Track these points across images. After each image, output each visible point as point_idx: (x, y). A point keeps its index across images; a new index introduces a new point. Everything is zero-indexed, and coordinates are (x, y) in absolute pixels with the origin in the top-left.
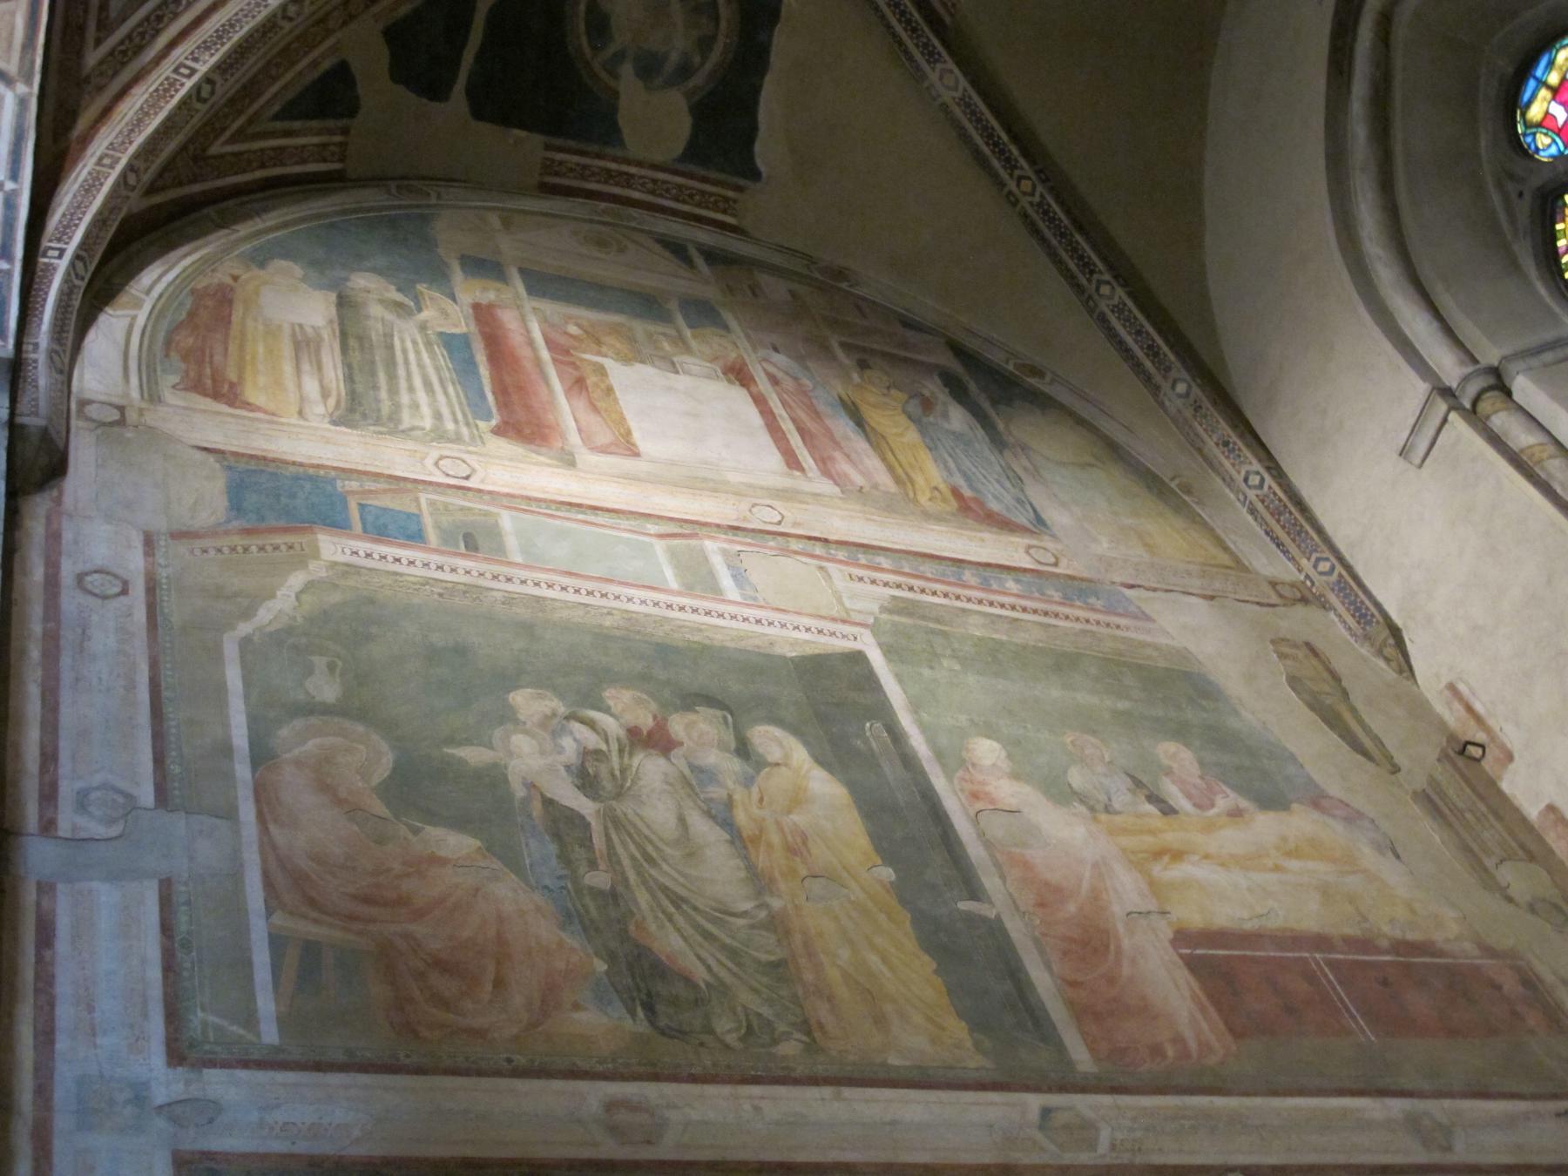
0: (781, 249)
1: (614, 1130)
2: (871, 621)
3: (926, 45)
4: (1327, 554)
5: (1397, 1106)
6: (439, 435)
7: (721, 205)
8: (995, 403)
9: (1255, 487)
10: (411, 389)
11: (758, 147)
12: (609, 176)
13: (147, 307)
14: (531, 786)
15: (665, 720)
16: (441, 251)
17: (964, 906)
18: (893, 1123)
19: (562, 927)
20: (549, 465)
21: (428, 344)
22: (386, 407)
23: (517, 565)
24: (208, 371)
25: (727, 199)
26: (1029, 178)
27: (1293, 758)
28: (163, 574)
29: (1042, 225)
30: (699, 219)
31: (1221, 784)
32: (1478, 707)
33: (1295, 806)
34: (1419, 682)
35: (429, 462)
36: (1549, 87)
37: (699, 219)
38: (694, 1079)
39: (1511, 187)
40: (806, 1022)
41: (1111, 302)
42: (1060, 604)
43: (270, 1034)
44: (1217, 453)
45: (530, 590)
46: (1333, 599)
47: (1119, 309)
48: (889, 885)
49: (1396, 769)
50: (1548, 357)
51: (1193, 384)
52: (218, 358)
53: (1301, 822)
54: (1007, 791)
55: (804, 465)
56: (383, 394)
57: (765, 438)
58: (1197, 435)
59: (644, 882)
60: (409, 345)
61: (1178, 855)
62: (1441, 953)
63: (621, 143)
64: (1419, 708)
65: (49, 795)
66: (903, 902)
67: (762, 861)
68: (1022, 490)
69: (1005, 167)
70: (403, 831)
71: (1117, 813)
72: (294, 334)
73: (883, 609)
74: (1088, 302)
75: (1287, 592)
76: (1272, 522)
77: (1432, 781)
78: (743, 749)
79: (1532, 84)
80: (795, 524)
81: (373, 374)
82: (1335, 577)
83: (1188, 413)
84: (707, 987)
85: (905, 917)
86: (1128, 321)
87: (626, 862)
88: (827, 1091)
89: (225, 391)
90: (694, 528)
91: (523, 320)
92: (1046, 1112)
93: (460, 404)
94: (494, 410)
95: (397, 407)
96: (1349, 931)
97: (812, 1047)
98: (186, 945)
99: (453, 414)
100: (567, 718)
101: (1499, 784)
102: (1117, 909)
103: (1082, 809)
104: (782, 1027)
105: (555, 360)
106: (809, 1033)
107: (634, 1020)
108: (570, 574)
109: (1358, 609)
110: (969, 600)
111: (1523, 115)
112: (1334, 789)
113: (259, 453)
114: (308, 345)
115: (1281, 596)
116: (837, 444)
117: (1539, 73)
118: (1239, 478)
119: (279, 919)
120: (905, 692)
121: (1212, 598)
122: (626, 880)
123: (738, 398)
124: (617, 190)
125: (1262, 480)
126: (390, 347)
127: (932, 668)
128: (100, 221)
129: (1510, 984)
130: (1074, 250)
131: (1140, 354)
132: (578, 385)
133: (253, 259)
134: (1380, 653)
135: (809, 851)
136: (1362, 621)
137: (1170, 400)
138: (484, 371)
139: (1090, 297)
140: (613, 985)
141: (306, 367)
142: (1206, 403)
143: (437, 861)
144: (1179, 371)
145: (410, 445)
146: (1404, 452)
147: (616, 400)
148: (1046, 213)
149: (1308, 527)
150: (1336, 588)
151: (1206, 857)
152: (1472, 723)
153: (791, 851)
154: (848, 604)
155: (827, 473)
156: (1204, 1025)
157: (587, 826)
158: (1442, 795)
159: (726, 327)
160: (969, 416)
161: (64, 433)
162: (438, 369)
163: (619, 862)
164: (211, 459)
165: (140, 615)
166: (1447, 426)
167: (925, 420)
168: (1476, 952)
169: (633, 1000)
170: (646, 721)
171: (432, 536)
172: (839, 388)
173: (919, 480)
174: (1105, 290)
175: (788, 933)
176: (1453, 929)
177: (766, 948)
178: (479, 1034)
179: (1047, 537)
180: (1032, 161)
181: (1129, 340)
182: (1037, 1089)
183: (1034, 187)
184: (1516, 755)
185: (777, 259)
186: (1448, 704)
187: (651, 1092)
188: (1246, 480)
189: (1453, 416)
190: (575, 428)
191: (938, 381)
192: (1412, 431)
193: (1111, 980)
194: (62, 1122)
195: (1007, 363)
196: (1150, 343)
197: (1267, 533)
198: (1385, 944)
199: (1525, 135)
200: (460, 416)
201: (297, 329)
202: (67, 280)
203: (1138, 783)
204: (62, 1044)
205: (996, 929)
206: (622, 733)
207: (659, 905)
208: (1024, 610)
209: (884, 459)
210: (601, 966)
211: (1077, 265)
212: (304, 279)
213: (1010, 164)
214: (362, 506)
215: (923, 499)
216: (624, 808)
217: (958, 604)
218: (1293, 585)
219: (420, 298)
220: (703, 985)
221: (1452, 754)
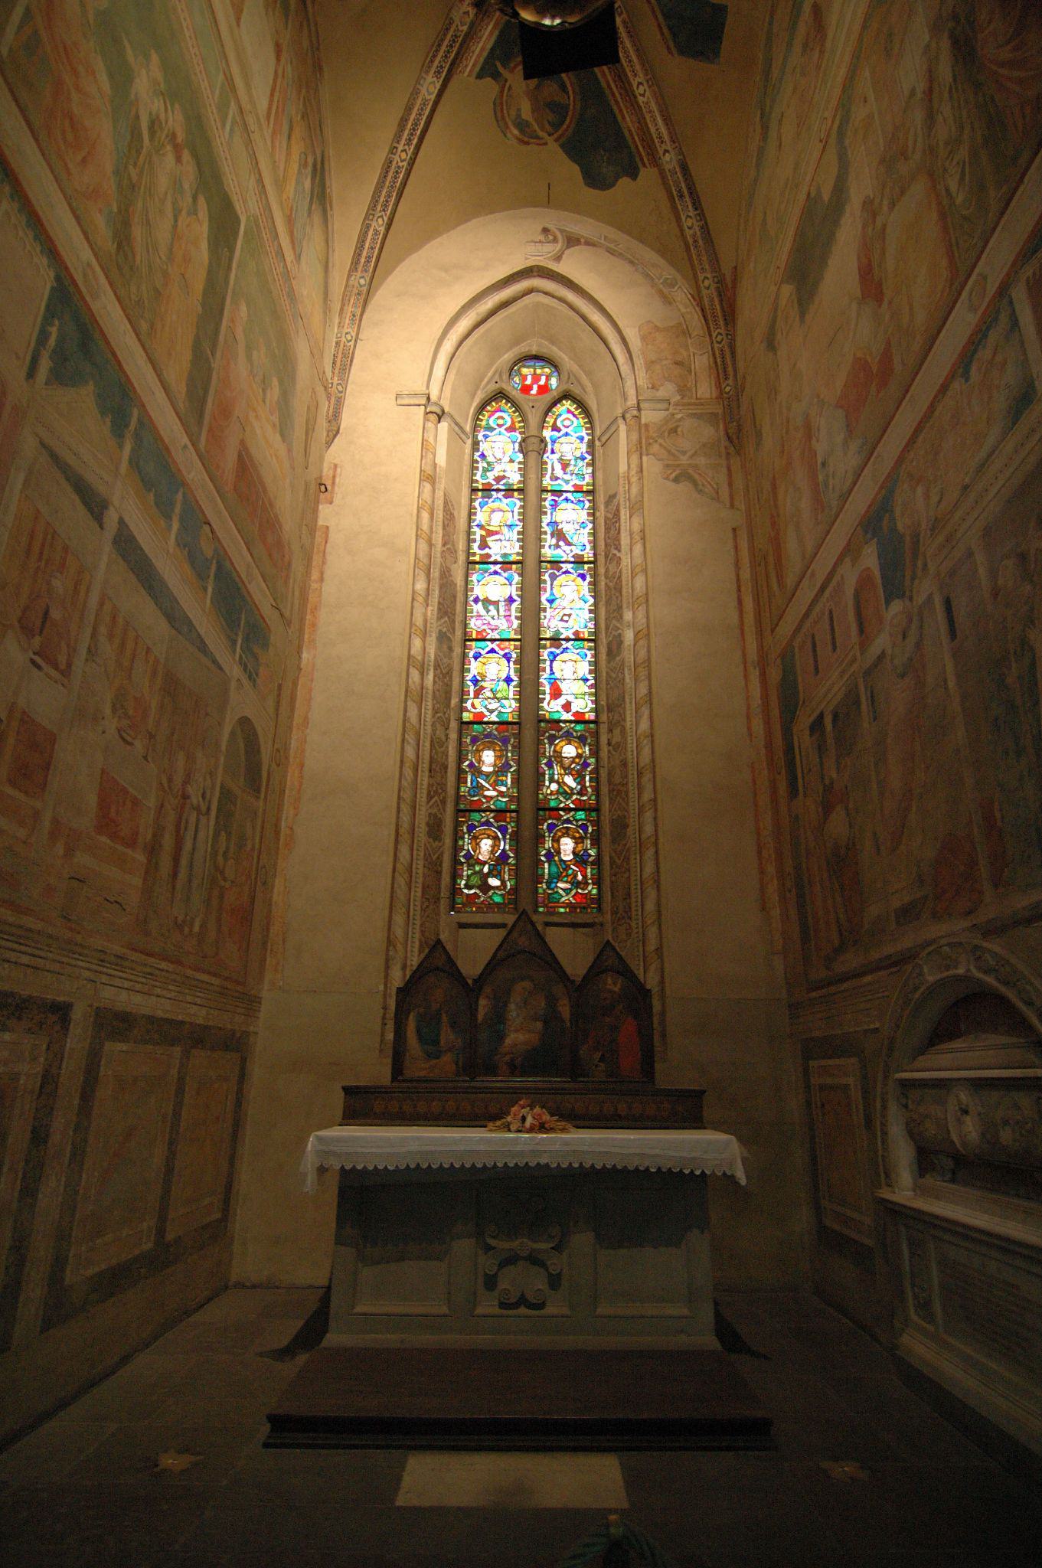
3: (441, 67)
29: (391, 174)
32: (337, 480)
36: (535, 371)
39: (497, 378)
46: (333, 399)
47: (376, 232)
50: (456, 428)
76: (340, 355)
79: (532, 364)
111: (521, 367)
134: (328, 432)
146: (398, 396)
186: (330, 468)
188: (347, 334)
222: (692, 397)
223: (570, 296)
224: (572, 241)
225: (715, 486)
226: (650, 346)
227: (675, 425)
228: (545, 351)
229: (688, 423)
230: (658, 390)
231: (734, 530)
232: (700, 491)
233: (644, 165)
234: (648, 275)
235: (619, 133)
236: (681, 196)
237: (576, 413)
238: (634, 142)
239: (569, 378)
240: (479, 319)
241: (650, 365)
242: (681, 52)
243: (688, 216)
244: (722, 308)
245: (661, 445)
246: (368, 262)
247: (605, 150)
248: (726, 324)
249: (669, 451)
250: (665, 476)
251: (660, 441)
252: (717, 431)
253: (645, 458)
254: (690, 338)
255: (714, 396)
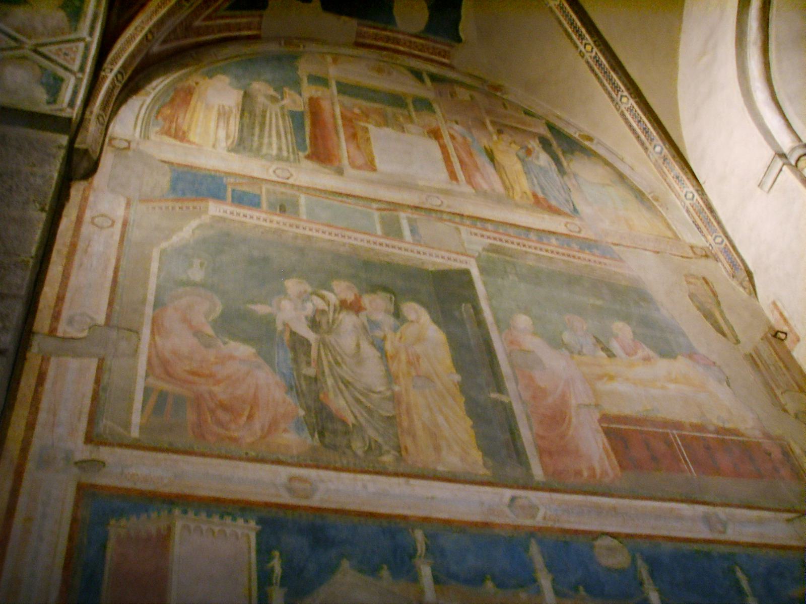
0: (471, 76)
1: (290, 490)
2: (477, 254)
4: (721, 234)
5: (701, 509)
6: (279, 158)
7: (443, 54)
8: (564, 152)
9: (690, 199)
10: (270, 136)
11: (461, 27)
12: (388, 39)
13: (152, 96)
14: (286, 325)
15: (360, 296)
16: (299, 72)
17: (494, 395)
18: (432, 498)
19: (287, 393)
20: (328, 174)
21: (283, 115)
22: (255, 145)
23: (304, 221)
24: (174, 125)
25: (445, 51)
26: (589, 44)
27: (684, 335)
28: (131, 218)
29: (596, 68)
30: (432, 61)
31: (642, 344)
32: (786, 314)
33: (679, 357)
34: (760, 300)
35: (271, 171)
37: (432, 61)
38: (336, 469)
40: (399, 447)
41: (627, 106)
42: (578, 251)
43: (135, 433)
44: (673, 182)
45: (308, 232)
46: (722, 257)
47: (630, 109)
48: (457, 384)
49: (738, 342)
51: (664, 147)
52: (180, 121)
53: (681, 365)
54: (532, 343)
55: (459, 179)
56: (256, 139)
57: (442, 165)
58: (664, 173)
59: (333, 375)
60: (274, 116)
61: (611, 378)
62: (743, 435)
63: (395, 23)
64: (757, 313)
65: (56, 317)
66: (463, 392)
67: (394, 367)
68: (570, 196)
69: (579, 39)
70: (220, 343)
71: (584, 355)
72: (219, 109)
73: (484, 249)
74: (617, 106)
75: (698, 251)
77: (757, 350)
78: (397, 314)
80: (448, 207)
81: (253, 128)
82: (723, 245)
83: (661, 161)
84: (353, 427)
85: (462, 400)
86: (635, 116)
87: (325, 363)
88: (402, 480)
89: (180, 135)
90: (395, 206)
91: (333, 104)
92: (513, 499)
93: (292, 144)
94: (308, 147)
95: (261, 145)
96: (695, 421)
97: (400, 458)
98: (105, 390)
99: (288, 148)
100: (312, 294)
101: (792, 352)
102: (573, 402)
103: (567, 353)
104: (385, 448)
105: (344, 125)
106: (400, 452)
107: (313, 439)
108: (329, 226)
109: (732, 262)
110: (530, 247)
112: (702, 350)
113: (190, 164)
114: (224, 115)
115: (694, 253)
116: (477, 167)
118: (682, 195)
119: (151, 380)
120: (487, 291)
121: (658, 252)
122: (324, 372)
123: (433, 146)
124: (392, 46)
125: (693, 196)
126: (264, 117)
127: (502, 278)
128: (133, 56)
129: (776, 454)
130: (610, 80)
131: (639, 131)
132: (353, 136)
133: (207, 75)
134: (741, 284)
135: (419, 364)
136: (734, 268)
137: (652, 155)
138: (308, 129)
139: (617, 103)
140: (305, 420)
141: (221, 124)
142: (669, 157)
143: (231, 357)
144: (657, 140)
145: (264, 162)
147: (370, 144)
148: (597, 61)
149: (713, 220)
150: (723, 251)
151: (627, 379)
152: (782, 322)
153: (409, 363)
154: (466, 245)
155: (470, 181)
156: (607, 463)
157: (310, 345)
158: (759, 356)
159: (434, 112)
160: (550, 159)
161: (98, 153)
162: (285, 128)
163: (322, 364)
164: (166, 166)
165: (117, 237)
166: (782, 173)
167: (526, 159)
168: (761, 436)
169: (314, 429)
170: (350, 297)
171: (264, 205)
172: (485, 142)
173: (517, 187)
174: (624, 100)
175: (399, 403)
176: (751, 424)
177: (387, 410)
178: (234, 440)
179: (577, 219)
180: (592, 36)
181: (634, 125)
182: (511, 487)
183: (592, 48)
184: (801, 339)
185: (468, 81)
186: (772, 311)
187: (312, 473)
188: (686, 196)
189: (785, 168)
190: (347, 156)
191: (538, 142)
192: (765, 175)
193: (562, 437)
194: (30, 466)
195: (575, 133)
196: (644, 126)
197: (693, 222)
198: (712, 428)
200: (291, 150)
201: (221, 107)
202: (113, 82)
203: (598, 341)
204: (38, 429)
205: (507, 410)
206: (337, 303)
207: (338, 386)
208: (558, 253)
209: (501, 178)
210: (302, 413)
211: (612, 88)
212: (230, 84)
213: (581, 37)
214: (233, 191)
215: (517, 198)
216: (330, 338)
217: (524, 249)
218: (702, 248)
219: (284, 94)
220: (351, 425)
221: (769, 336)
240: (759, 44)
246: (647, 132)
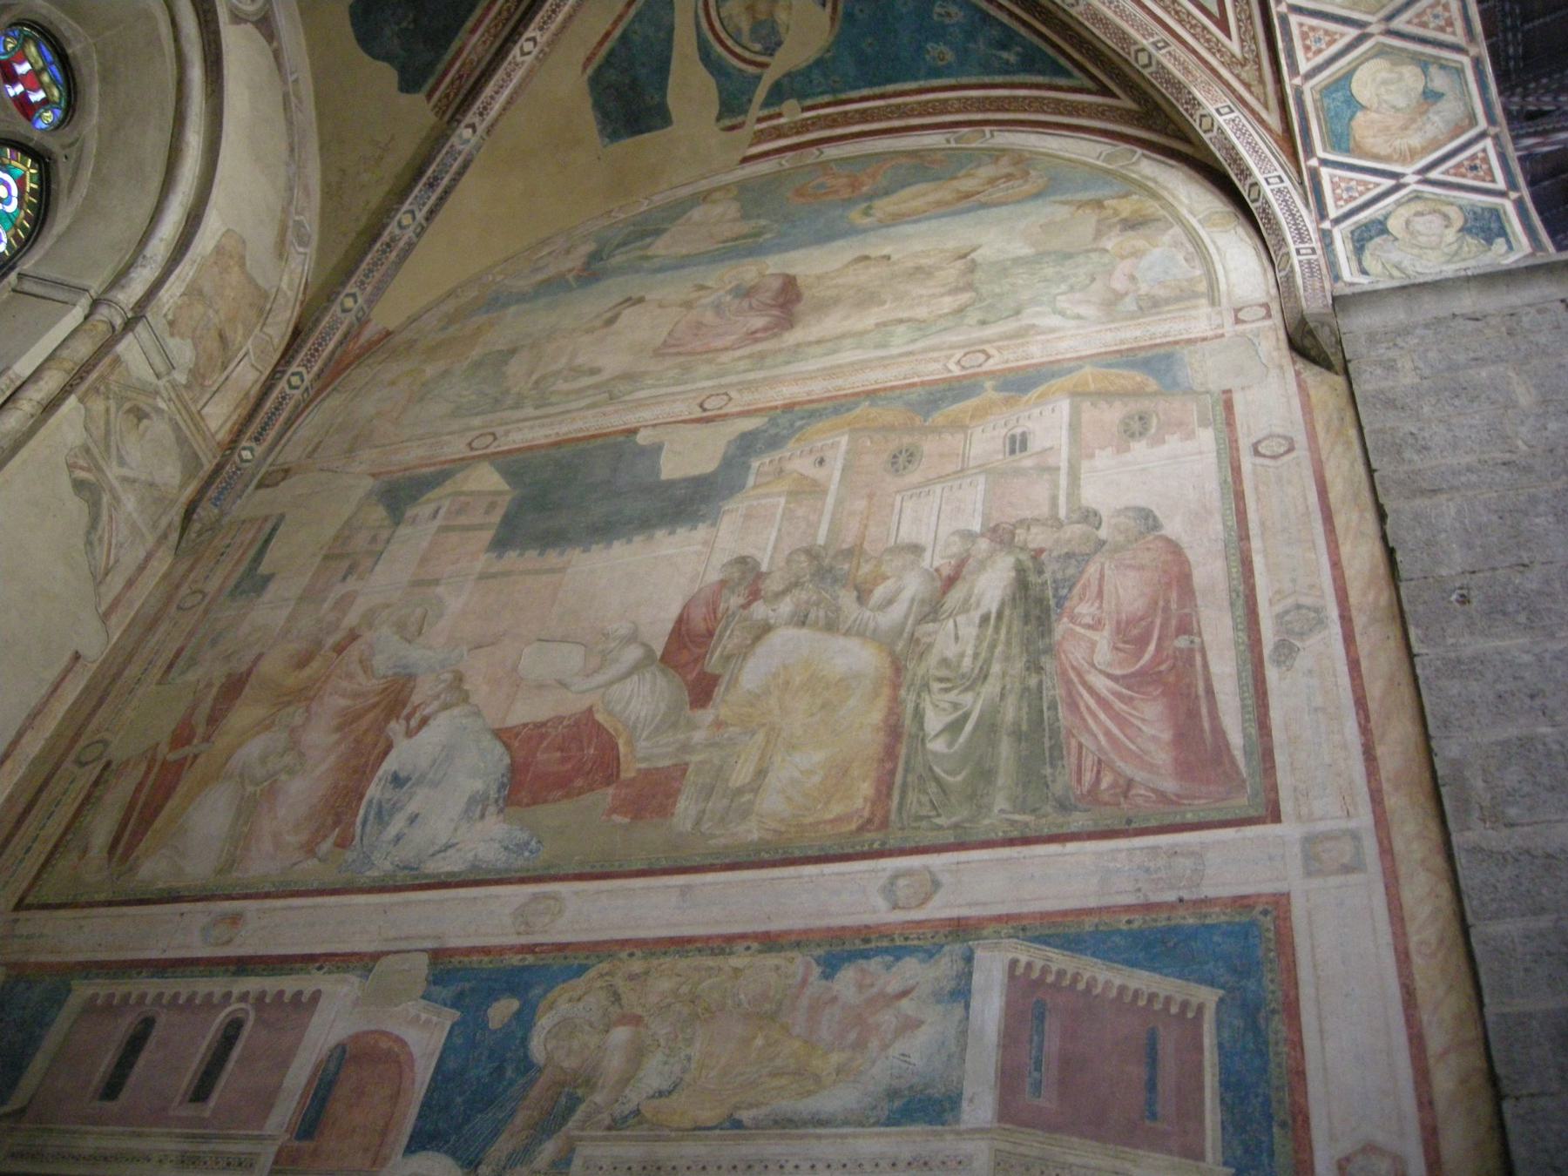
79: (50, 58)
117: (54, 68)
199: (21, 31)
222: (195, 401)
223: (196, 74)
224: (265, 24)
225: (112, 562)
226: (216, 269)
227: (147, 409)
228: (85, 71)
229: (159, 427)
230: (172, 335)
231: (77, 657)
232: (89, 543)
233: (429, 96)
234: (291, 189)
235: (450, 32)
236: (431, 185)
237: (28, 198)
238: (451, 64)
239: (72, 144)
241: (194, 292)
242: (594, 81)
243: (412, 212)
244: (333, 352)
245: (107, 410)
247: (415, 21)
248: (318, 376)
249: (108, 433)
250: (71, 461)
251: (112, 403)
252: (183, 486)
253: (72, 401)
254: (261, 330)
255: (219, 437)
